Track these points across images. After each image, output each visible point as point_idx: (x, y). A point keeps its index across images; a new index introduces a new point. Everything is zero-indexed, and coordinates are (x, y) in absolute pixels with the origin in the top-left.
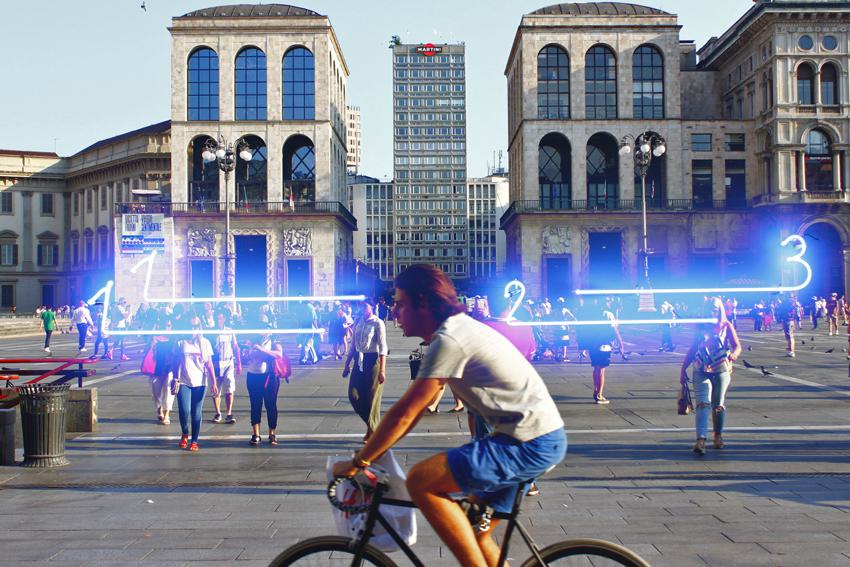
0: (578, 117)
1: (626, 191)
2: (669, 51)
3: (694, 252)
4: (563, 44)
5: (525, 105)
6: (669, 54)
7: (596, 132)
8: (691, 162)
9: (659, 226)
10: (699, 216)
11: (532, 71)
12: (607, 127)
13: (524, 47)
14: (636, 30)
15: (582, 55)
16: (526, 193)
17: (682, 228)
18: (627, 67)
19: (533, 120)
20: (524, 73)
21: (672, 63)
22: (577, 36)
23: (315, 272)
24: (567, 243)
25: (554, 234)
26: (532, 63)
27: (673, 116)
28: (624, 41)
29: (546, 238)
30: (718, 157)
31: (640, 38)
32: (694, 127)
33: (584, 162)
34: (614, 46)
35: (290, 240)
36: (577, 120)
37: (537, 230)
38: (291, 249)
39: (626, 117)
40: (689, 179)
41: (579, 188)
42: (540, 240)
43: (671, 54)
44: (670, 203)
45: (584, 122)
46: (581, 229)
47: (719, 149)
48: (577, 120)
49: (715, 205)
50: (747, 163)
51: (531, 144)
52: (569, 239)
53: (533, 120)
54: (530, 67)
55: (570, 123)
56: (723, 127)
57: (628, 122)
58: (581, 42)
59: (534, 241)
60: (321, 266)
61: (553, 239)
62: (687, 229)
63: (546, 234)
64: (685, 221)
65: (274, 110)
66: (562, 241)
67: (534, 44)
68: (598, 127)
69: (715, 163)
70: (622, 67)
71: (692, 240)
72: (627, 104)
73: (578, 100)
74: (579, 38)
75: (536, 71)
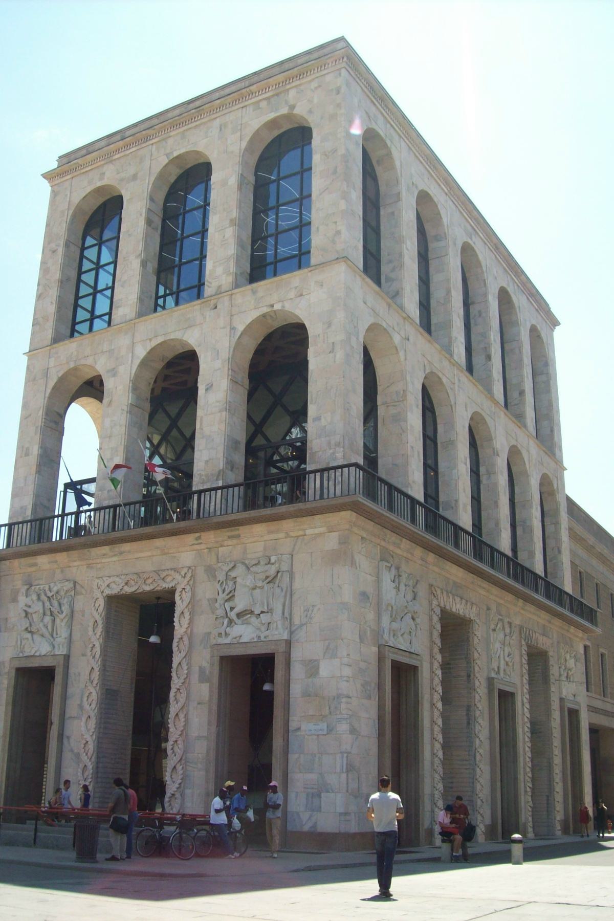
23: (296, 689)
38: (231, 622)
60: (312, 668)
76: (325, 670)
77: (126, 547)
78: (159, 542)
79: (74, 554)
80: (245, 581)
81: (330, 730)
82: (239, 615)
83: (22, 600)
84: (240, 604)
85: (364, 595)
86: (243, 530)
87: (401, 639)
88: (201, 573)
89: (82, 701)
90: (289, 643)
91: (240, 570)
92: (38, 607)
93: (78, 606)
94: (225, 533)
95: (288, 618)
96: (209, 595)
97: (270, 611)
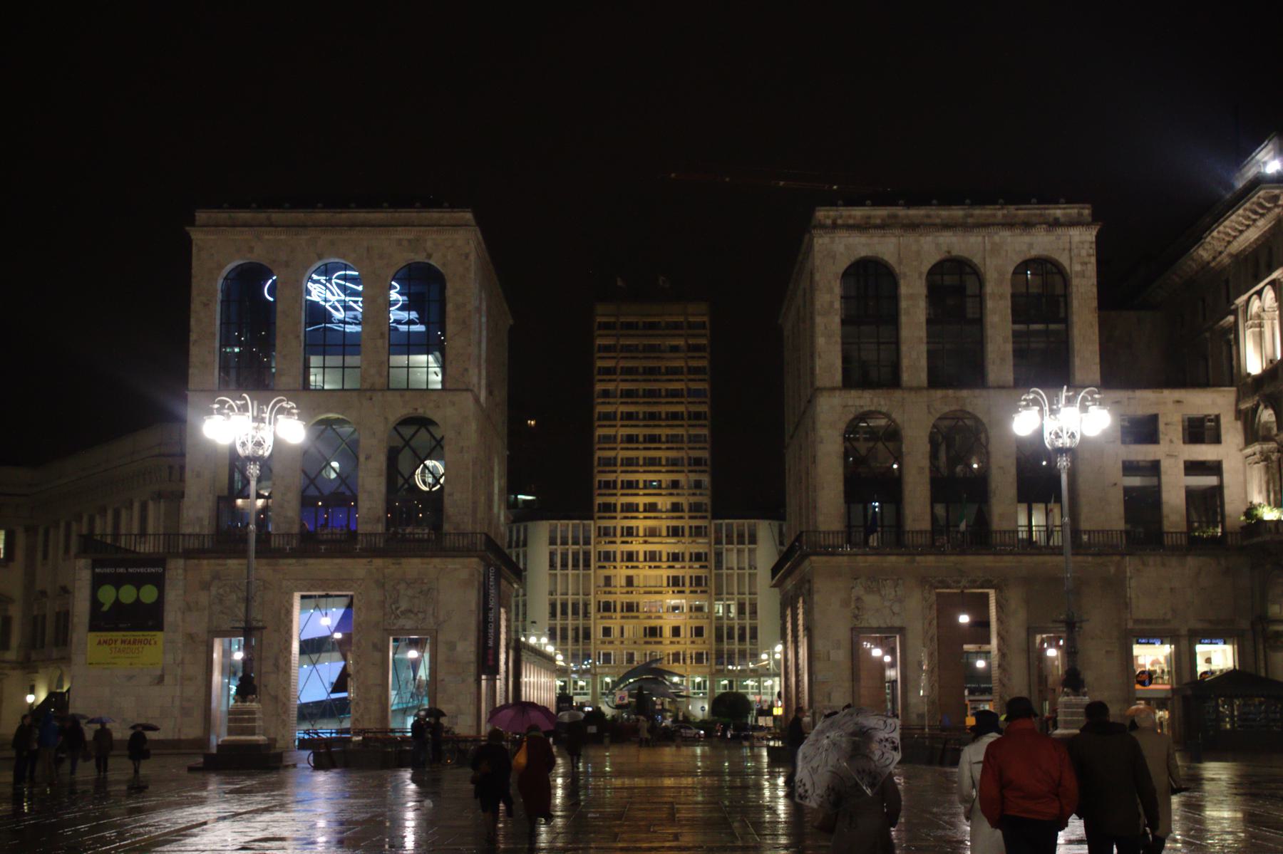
0: (915, 384)
2: (1077, 268)
3: (1130, 625)
4: (886, 258)
5: (818, 363)
6: (1077, 273)
8: (1120, 465)
11: (831, 304)
13: (817, 262)
15: (920, 276)
16: (821, 518)
18: (1001, 297)
19: (833, 389)
20: (818, 305)
22: (910, 240)
24: (896, 608)
25: (869, 590)
26: (831, 291)
30: (1170, 456)
31: (1025, 248)
33: (925, 463)
34: (977, 260)
35: (396, 601)
36: (911, 389)
42: (845, 603)
43: (1082, 274)
44: (1085, 538)
45: (925, 392)
46: (924, 581)
47: (1171, 441)
48: (911, 389)
49: (1167, 540)
50: (1225, 466)
52: (901, 601)
53: (833, 389)
54: (827, 297)
55: (898, 394)
56: (1178, 402)
60: (452, 646)
61: (871, 600)
63: (859, 591)
65: (373, 371)
67: (834, 257)
69: (1165, 465)
72: (1003, 360)
74: (914, 248)
75: (837, 305)
81: (463, 681)
82: (403, 613)
83: (214, 590)
84: (404, 605)
89: (276, 659)
91: (402, 587)
97: (424, 612)
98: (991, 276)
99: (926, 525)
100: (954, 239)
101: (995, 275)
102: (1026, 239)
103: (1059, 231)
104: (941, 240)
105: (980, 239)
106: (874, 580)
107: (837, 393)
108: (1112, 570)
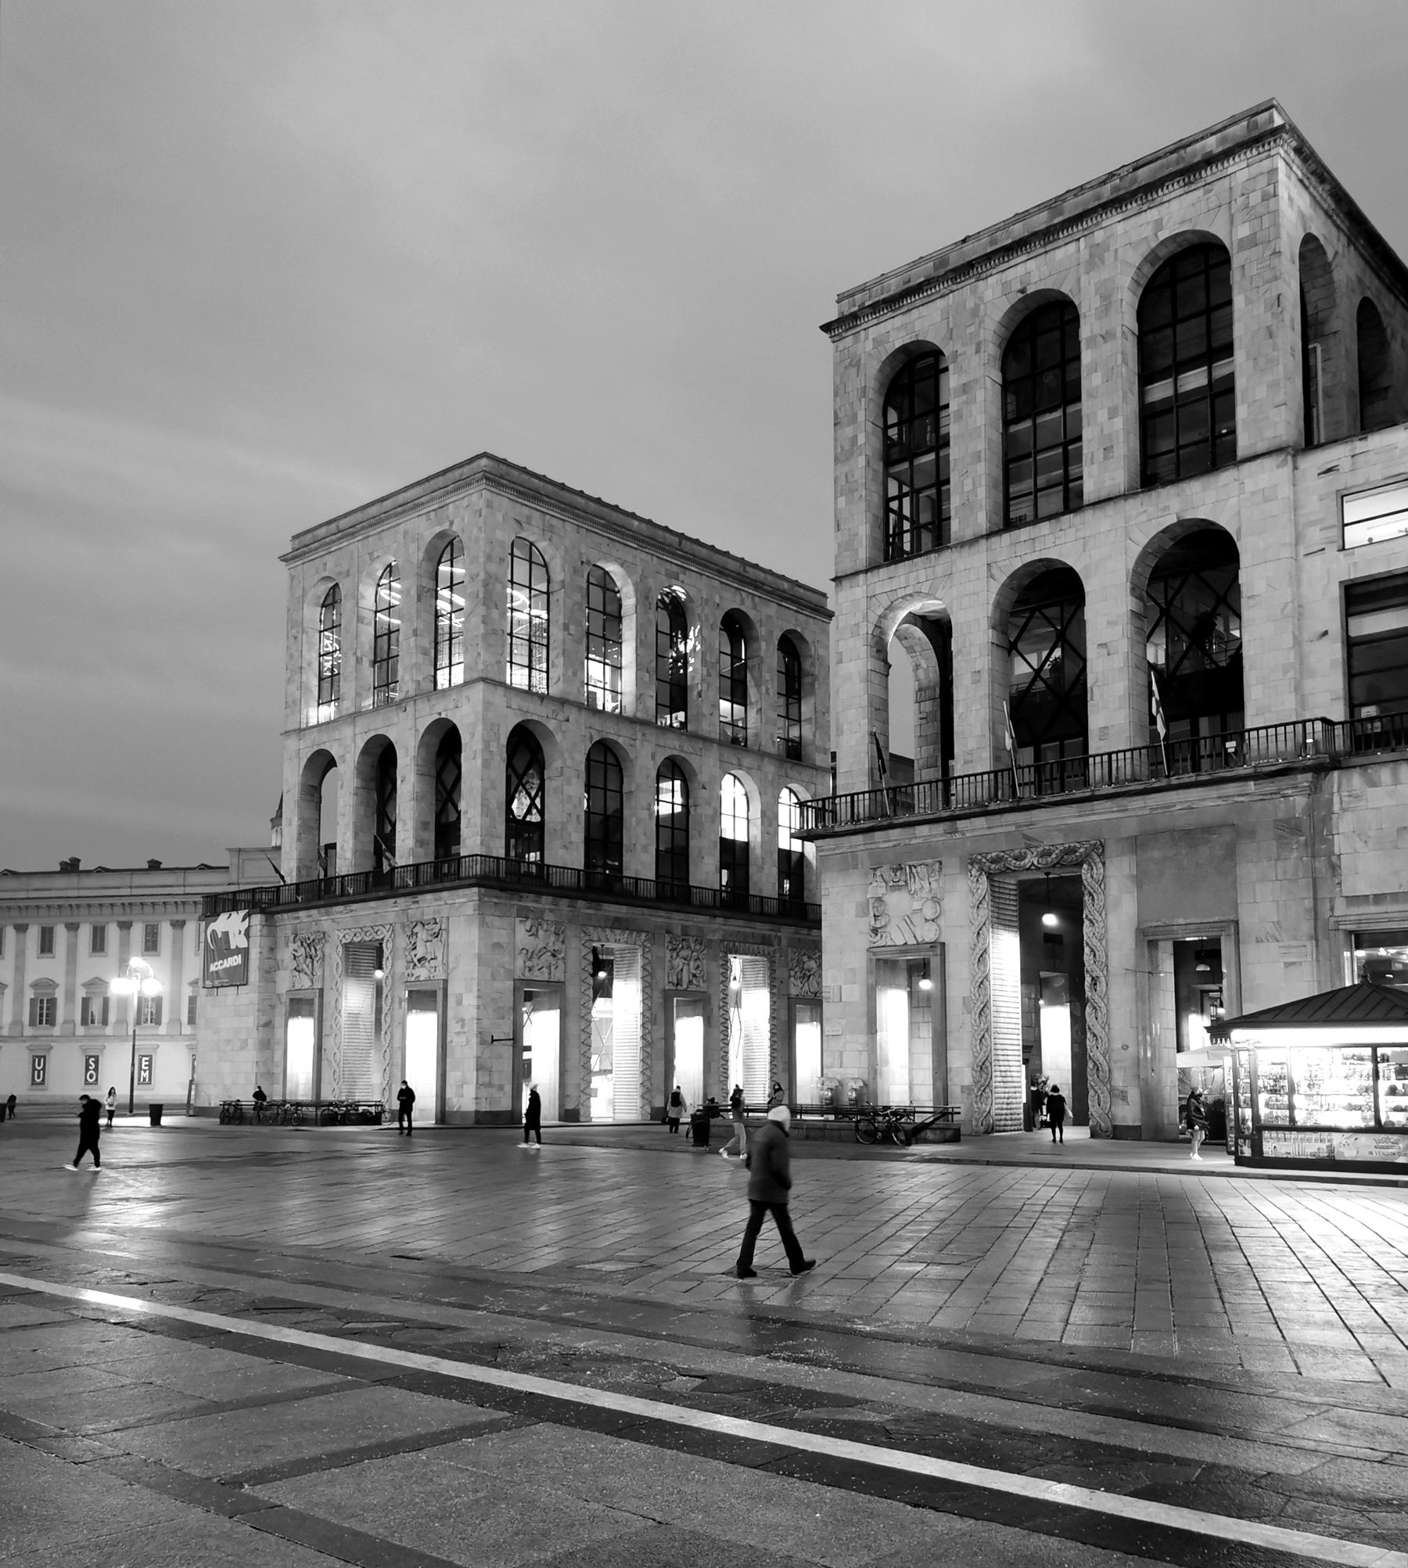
0: (969, 534)
1: (1104, 730)
2: (1243, 231)
7: (1018, 564)
8: (1336, 593)
9: (1208, 830)
10: (1356, 779)
11: (855, 438)
12: (1050, 540)
14: (1133, 207)
17: (1289, 828)
19: (856, 573)
21: (1252, 270)
25: (896, 887)
27: (1261, 447)
28: (1096, 258)
29: (879, 899)
31: (1148, 231)
32: (1345, 464)
37: (855, 878)
39: (1104, 495)
40: (1333, 652)
41: (972, 744)
45: (983, 543)
51: (851, 642)
53: (856, 573)
57: (1110, 508)
58: (975, 311)
59: (850, 910)
60: (459, 1002)
62: (1312, 834)
63: (878, 889)
64: (1301, 801)
66: (917, 905)
67: (858, 365)
68: (1021, 549)
70: (1092, 340)
71: (1334, 868)
73: (968, 487)
74: (970, 304)
76: (465, 1002)
77: (354, 906)
78: (372, 904)
79: (323, 910)
80: (422, 934)
82: (419, 961)
83: (292, 946)
85: (498, 945)
86: (420, 897)
87: (537, 973)
88: (398, 926)
90: (446, 981)
92: (302, 951)
93: (327, 952)
94: (409, 899)
95: (446, 964)
96: (404, 945)
98: (1088, 306)
99: (984, 764)
100: (1031, 265)
101: (1096, 302)
102: (1153, 215)
103: (1208, 175)
104: (1011, 274)
105: (1072, 247)
106: (899, 869)
107: (862, 577)
108: (1301, 801)
